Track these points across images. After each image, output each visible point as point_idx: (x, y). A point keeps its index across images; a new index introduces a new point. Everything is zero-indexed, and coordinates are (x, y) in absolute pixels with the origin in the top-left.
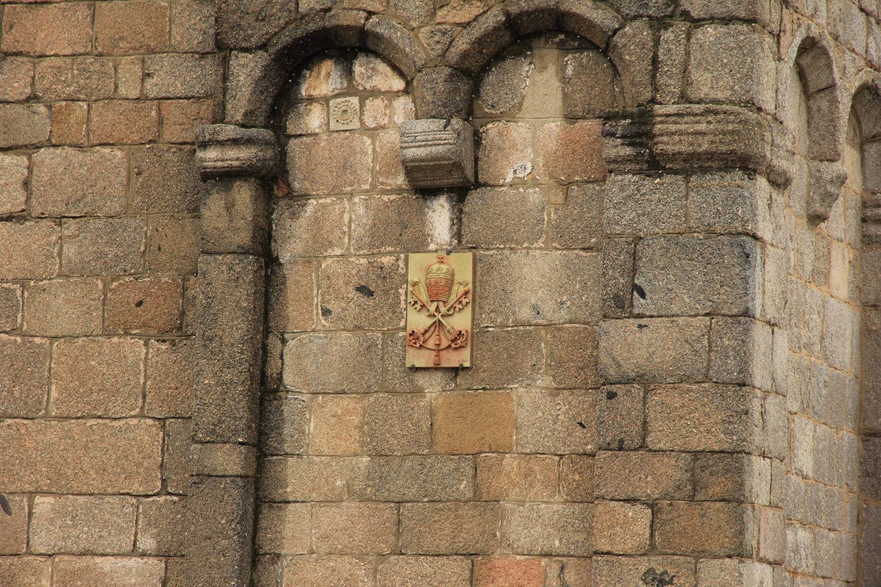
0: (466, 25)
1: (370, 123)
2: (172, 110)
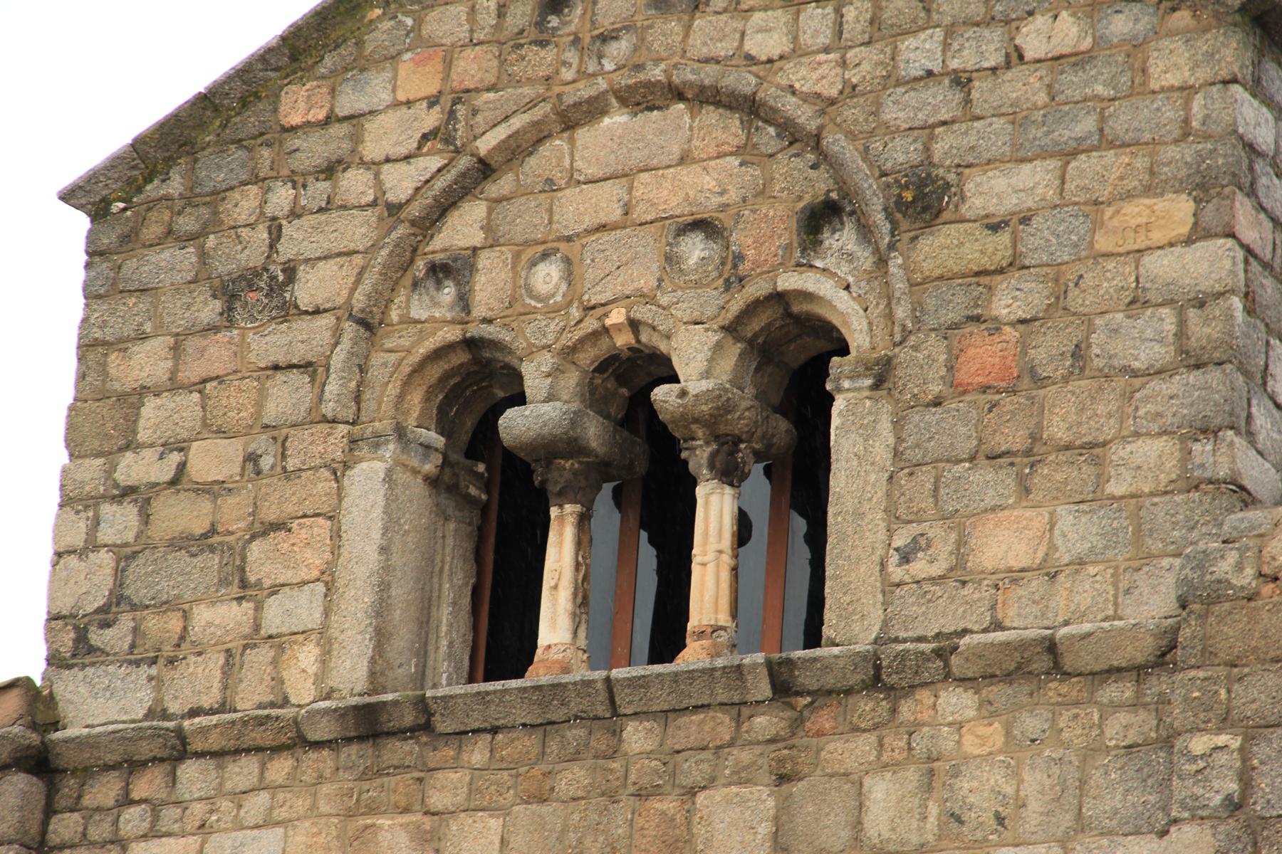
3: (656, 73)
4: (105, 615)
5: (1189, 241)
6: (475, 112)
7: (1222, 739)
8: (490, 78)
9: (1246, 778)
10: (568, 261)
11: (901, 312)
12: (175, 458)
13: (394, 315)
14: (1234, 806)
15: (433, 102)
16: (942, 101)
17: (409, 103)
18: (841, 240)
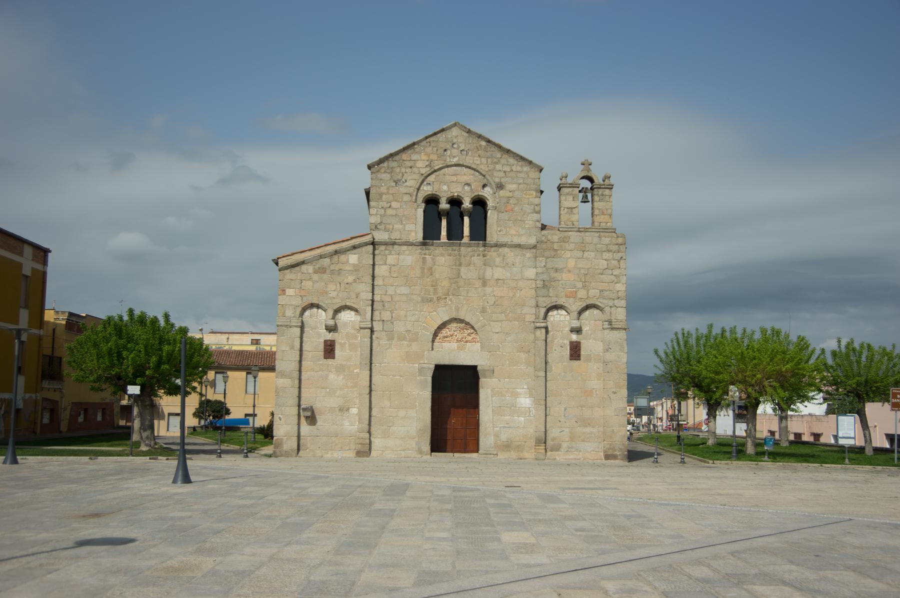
1: (561, 320)
3: (461, 163)
4: (381, 223)
5: (535, 198)
7: (543, 258)
9: (546, 263)
10: (448, 186)
11: (498, 200)
12: (389, 204)
13: (421, 188)
14: (545, 266)
15: (428, 160)
16: (502, 174)
18: (487, 189)
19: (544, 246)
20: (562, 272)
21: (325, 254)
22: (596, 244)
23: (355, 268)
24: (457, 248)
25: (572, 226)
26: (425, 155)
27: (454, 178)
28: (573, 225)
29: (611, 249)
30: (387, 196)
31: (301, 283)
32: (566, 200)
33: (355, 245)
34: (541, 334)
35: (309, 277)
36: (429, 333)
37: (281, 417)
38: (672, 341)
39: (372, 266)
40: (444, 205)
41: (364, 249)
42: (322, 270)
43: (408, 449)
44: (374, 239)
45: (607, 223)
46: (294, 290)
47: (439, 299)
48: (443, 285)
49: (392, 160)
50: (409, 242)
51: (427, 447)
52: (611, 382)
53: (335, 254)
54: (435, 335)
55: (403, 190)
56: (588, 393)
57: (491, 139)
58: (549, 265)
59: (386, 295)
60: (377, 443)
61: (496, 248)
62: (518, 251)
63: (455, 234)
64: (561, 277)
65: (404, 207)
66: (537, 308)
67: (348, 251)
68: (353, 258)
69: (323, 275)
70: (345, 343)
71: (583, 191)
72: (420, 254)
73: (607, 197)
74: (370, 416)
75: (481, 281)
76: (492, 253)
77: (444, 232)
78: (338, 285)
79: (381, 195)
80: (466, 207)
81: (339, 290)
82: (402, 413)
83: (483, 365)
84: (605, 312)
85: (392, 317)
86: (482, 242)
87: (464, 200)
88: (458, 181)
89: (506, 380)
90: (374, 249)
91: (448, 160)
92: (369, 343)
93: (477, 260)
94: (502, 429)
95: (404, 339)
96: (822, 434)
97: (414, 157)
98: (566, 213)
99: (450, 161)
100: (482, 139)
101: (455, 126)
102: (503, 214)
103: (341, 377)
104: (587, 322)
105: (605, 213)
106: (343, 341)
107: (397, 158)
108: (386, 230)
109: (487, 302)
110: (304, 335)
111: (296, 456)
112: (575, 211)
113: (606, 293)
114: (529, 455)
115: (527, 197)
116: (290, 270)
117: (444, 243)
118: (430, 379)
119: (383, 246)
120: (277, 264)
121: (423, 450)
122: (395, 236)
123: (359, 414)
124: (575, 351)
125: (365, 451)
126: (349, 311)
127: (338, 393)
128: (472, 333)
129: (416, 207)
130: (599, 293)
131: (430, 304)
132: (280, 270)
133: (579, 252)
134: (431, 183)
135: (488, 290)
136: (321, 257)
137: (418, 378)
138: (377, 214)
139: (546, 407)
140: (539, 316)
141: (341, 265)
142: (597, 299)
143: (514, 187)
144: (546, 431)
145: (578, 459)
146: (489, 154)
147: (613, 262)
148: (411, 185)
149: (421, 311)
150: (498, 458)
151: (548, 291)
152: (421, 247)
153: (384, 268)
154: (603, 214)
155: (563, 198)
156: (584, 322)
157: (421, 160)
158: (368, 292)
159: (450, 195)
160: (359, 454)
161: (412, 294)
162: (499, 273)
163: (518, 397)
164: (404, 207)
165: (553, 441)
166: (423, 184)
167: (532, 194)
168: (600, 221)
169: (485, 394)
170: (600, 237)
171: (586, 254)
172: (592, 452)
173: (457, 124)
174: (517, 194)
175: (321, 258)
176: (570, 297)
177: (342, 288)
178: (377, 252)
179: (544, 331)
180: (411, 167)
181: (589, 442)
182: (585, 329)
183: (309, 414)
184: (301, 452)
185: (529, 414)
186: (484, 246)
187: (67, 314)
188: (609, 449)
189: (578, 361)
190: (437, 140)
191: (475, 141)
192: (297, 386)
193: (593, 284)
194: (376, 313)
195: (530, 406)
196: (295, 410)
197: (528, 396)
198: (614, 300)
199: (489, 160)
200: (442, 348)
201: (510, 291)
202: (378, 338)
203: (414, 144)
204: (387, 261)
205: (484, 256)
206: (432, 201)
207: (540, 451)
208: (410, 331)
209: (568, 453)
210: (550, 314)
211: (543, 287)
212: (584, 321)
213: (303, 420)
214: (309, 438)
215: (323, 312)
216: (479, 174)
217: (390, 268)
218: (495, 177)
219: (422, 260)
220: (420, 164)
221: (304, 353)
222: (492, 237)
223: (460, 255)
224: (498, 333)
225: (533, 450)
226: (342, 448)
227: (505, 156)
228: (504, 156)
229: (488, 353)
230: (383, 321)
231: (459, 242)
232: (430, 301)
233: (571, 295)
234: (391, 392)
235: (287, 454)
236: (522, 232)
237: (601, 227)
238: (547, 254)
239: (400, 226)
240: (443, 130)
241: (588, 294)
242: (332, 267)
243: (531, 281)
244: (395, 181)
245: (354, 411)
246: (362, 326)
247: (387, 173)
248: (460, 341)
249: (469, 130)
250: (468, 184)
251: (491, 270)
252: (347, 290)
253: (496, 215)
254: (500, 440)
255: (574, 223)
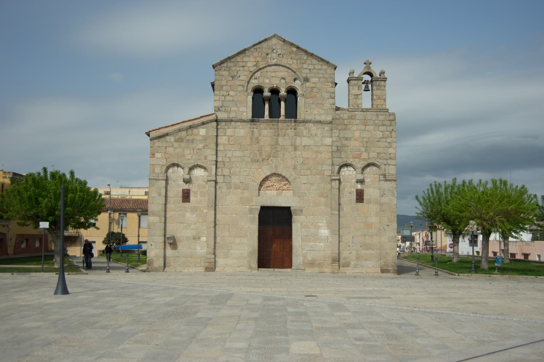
0: (363, 164)
1: (350, 174)
2: (326, 172)
3: (279, 63)
4: (222, 107)
5: (331, 88)
6: (259, 64)
8: (261, 60)
11: (305, 90)
13: (250, 82)
14: (338, 136)
15: (255, 62)
16: (308, 71)
17: (252, 62)
18: (297, 82)
19: (338, 122)
20: (351, 140)
21: (182, 129)
22: (374, 121)
23: (204, 138)
24: (276, 124)
25: (357, 108)
26: (253, 57)
27: (274, 74)
28: (358, 107)
29: (385, 123)
30: (227, 87)
31: (166, 149)
32: (353, 89)
33: (203, 122)
34: (335, 184)
35: (171, 145)
36: (256, 184)
37: (152, 244)
38: (428, 190)
39: (216, 137)
40: (267, 94)
41: (210, 124)
42: (181, 140)
43: (242, 266)
44: (217, 117)
45: (382, 105)
46: (161, 154)
47: (263, 160)
48: (266, 150)
49: (230, 61)
50: (242, 119)
51: (255, 264)
52: (386, 218)
53: (190, 129)
54: (261, 185)
55: (237, 82)
56: (370, 226)
57: (300, 46)
58: (342, 135)
59: (226, 157)
60: (220, 261)
61: (304, 123)
62: (319, 126)
63: (274, 114)
64: (349, 144)
65: (239, 95)
66: (333, 166)
67: (199, 126)
68: (202, 131)
69: (181, 143)
70: (197, 191)
71: (366, 82)
72: (250, 128)
73: (382, 87)
74: (215, 243)
75: (293, 147)
76: (301, 127)
77: (267, 113)
78: (192, 150)
79: (222, 87)
80: (282, 95)
81: (192, 154)
82: (237, 241)
83: (295, 207)
84: (381, 169)
85: (230, 173)
86: (293, 119)
87: (281, 90)
88: (276, 76)
89: (311, 217)
90: (217, 125)
91: (269, 62)
92: (214, 191)
93: (291, 132)
94: (308, 252)
95: (239, 188)
96: (530, 254)
97: (246, 59)
98: (353, 99)
99: (271, 62)
100: (293, 46)
101: (274, 37)
102: (308, 99)
103: (195, 215)
104: (368, 176)
105: (381, 98)
106: (195, 190)
107: (233, 60)
108: (226, 111)
109: (298, 162)
110: (169, 186)
111: (163, 271)
112: (359, 97)
113: (382, 155)
114: (327, 270)
115: (326, 87)
116: (158, 140)
117: (267, 120)
118: (257, 216)
119: (224, 123)
120: (149, 135)
121: (253, 267)
122: (232, 115)
123: (207, 242)
124: (360, 196)
125: (211, 268)
126: (200, 168)
127: (192, 227)
128: (287, 184)
129: (247, 95)
130: (376, 155)
131: (257, 163)
132: (151, 140)
133: (362, 126)
134: (258, 78)
135: (298, 153)
136: (180, 130)
137: (249, 216)
138: (219, 100)
139: (339, 236)
140: (334, 172)
141: (194, 136)
142: (376, 159)
143: (316, 80)
144: (339, 253)
145: (362, 273)
146: (298, 57)
147: (386, 133)
148: (243, 79)
149: (250, 169)
150: (306, 272)
151: (341, 154)
152: (251, 123)
153: (224, 138)
154: (380, 99)
155: (351, 88)
156: (366, 176)
157: (250, 61)
158: (213, 155)
159: (271, 86)
160: (207, 269)
161: (244, 156)
162: (306, 141)
163: (320, 229)
164: (239, 95)
165: (344, 260)
166: (252, 79)
167: (329, 85)
168: (377, 104)
169: (296, 227)
170: (377, 115)
171: (367, 127)
172: (372, 268)
173: (276, 35)
174: (318, 85)
175: (180, 131)
176: (356, 158)
177: (194, 152)
178: (219, 127)
179: (337, 182)
180: (243, 67)
181: (370, 260)
182: (367, 180)
183: (171, 241)
184: (166, 269)
185: (328, 241)
186: (295, 122)
187: (12, 174)
188: (384, 265)
189: (362, 203)
190: (261, 47)
191: (288, 47)
192: (163, 221)
193: (372, 149)
194: (219, 170)
195: (328, 235)
196: (162, 239)
197: (326, 228)
198: (387, 160)
199: (298, 61)
200: (266, 194)
201: (314, 154)
202: (220, 188)
203: (245, 50)
204: (227, 133)
205: (295, 129)
206: (258, 91)
207: (335, 267)
208: (242, 182)
209: (355, 268)
210: (342, 170)
211: (337, 151)
212: (366, 175)
213: (168, 245)
214: (172, 258)
215: (182, 170)
216: (291, 71)
217: (229, 138)
218: (303, 73)
219: (251, 132)
220: (249, 64)
221: (169, 198)
222: (300, 116)
223: (278, 129)
224: (305, 184)
225: (330, 267)
226: (195, 265)
227: (310, 58)
228: (309, 58)
229: (298, 198)
230: (224, 175)
231: (277, 119)
232: (257, 161)
233: (357, 156)
234: (230, 226)
235: (156, 270)
236: (322, 112)
237: (378, 108)
238: (340, 127)
239: (236, 109)
240: (265, 40)
241: (369, 155)
242: (188, 138)
243: (328, 147)
244: (231, 77)
245: (204, 239)
246: (209, 179)
247: (226, 70)
248: (279, 189)
249: (284, 40)
250: (284, 79)
251: (300, 139)
252: (198, 154)
253: (303, 100)
254: (307, 260)
255: (359, 105)
